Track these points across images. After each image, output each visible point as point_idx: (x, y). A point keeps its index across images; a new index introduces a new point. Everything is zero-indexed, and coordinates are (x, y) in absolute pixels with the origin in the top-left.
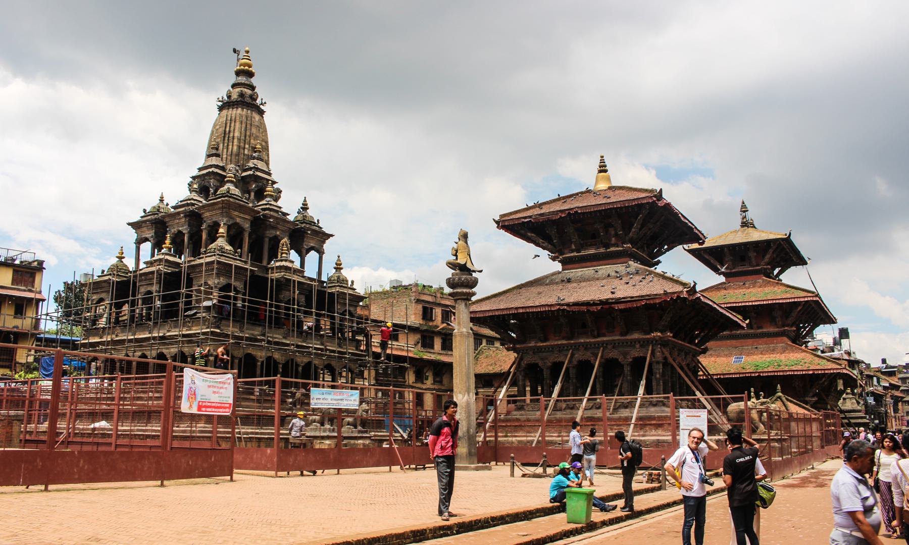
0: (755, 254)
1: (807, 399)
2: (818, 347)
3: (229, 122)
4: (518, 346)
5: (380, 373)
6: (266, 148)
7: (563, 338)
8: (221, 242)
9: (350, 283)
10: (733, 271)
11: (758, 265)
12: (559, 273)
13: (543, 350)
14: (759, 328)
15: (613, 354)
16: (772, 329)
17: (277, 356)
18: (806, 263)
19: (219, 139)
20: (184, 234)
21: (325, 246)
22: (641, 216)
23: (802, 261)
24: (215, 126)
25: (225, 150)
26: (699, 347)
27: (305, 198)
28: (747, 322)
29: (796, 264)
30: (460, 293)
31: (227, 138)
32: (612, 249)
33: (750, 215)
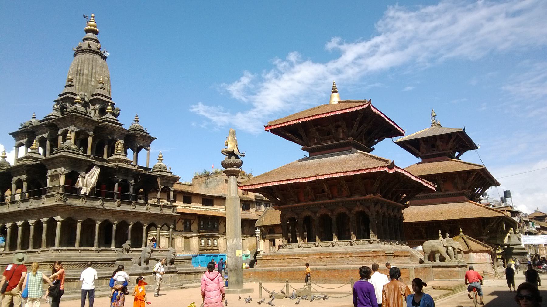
0: (441, 143)
2: (490, 203)
5: (201, 227)
7: (311, 200)
11: (443, 150)
13: (298, 208)
14: (446, 191)
15: (341, 210)
16: (455, 192)
18: (477, 148)
19: (74, 75)
22: (358, 118)
25: (78, 82)
26: (403, 204)
28: (436, 186)
29: (470, 149)
32: (341, 141)
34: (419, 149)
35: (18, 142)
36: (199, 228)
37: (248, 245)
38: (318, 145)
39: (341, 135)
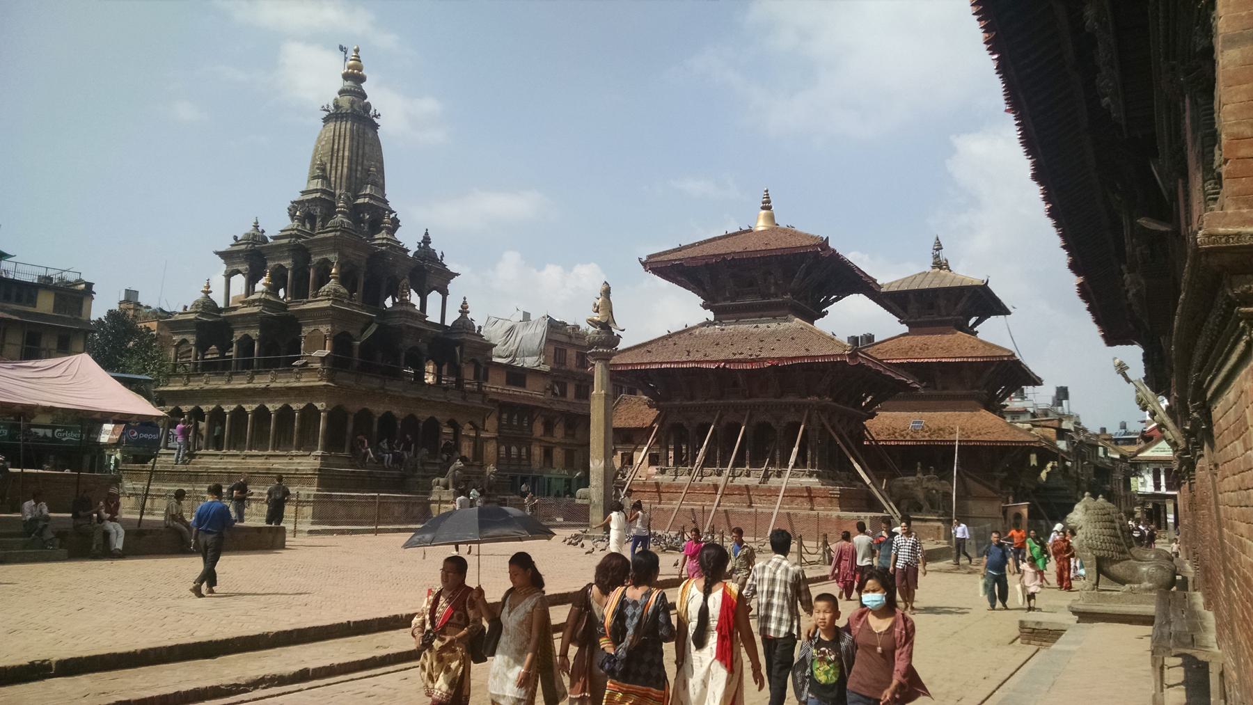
1: (996, 474)
3: (337, 138)
4: (661, 403)
5: (504, 425)
6: (381, 171)
8: (332, 284)
9: (477, 329)
10: (919, 320)
11: (948, 315)
14: (944, 388)
16: (960, 392)
17: (396, 411)
19: (326, 158)
20: (287, 270)
21: (449, 287)
22: (804, 265)
23: (1002, 310)
24: (319, 140)
25: (333, 172)
27: (427, 230)
31: (335, 158)
33: (944, 254)
34: (905, 309)
35: (230, 269)
36: (499, 426)
37: (582, 461)
38: (731, 302)
39: (773, 289)
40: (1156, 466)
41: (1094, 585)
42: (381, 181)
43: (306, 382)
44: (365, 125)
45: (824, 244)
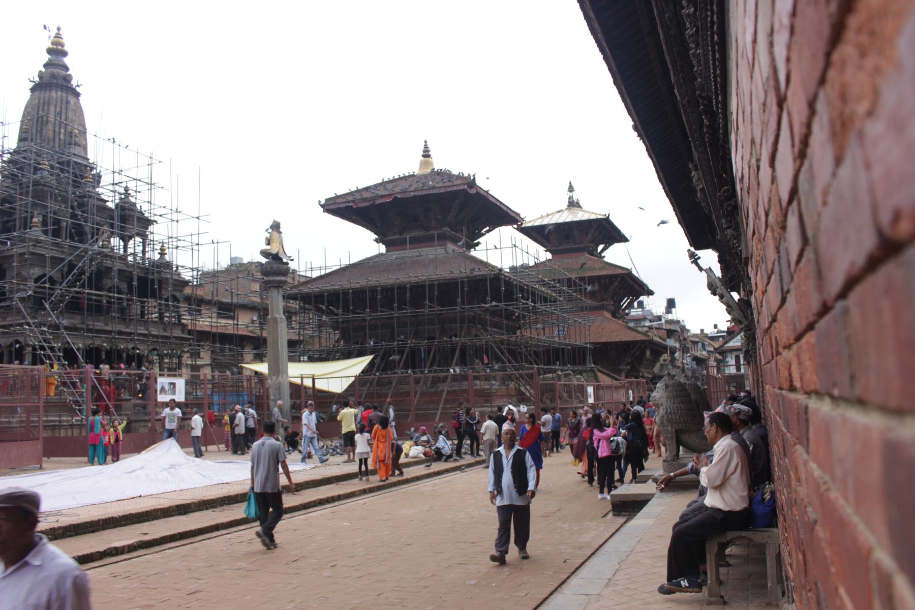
1: (621, 367)
2: (647, 317)
3: (41, 105)
10: (559, 248)
11: (581, 243)
12: (382, 255)
22: (457, 201)
23: (623, 239)
25: (39, 135)
30: (272, 281)
31: (39, 122)
33: (576, 196)
39: (433, 224)
40: (737, 353)
41: (674, 456)
42: (84, 142)
43: (11, 321)
44: (67, 94)
45: (471, 183)
